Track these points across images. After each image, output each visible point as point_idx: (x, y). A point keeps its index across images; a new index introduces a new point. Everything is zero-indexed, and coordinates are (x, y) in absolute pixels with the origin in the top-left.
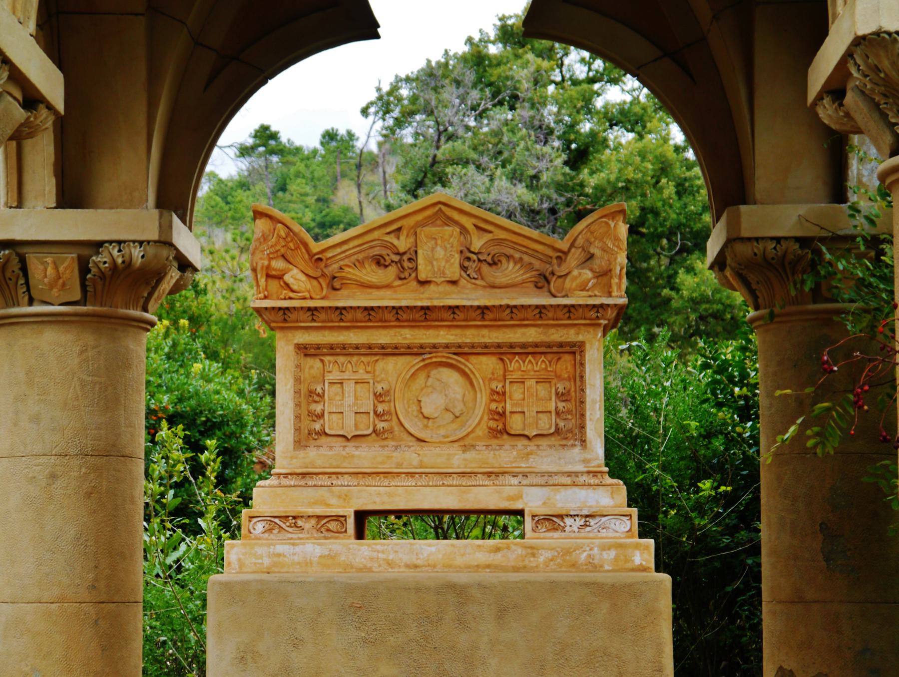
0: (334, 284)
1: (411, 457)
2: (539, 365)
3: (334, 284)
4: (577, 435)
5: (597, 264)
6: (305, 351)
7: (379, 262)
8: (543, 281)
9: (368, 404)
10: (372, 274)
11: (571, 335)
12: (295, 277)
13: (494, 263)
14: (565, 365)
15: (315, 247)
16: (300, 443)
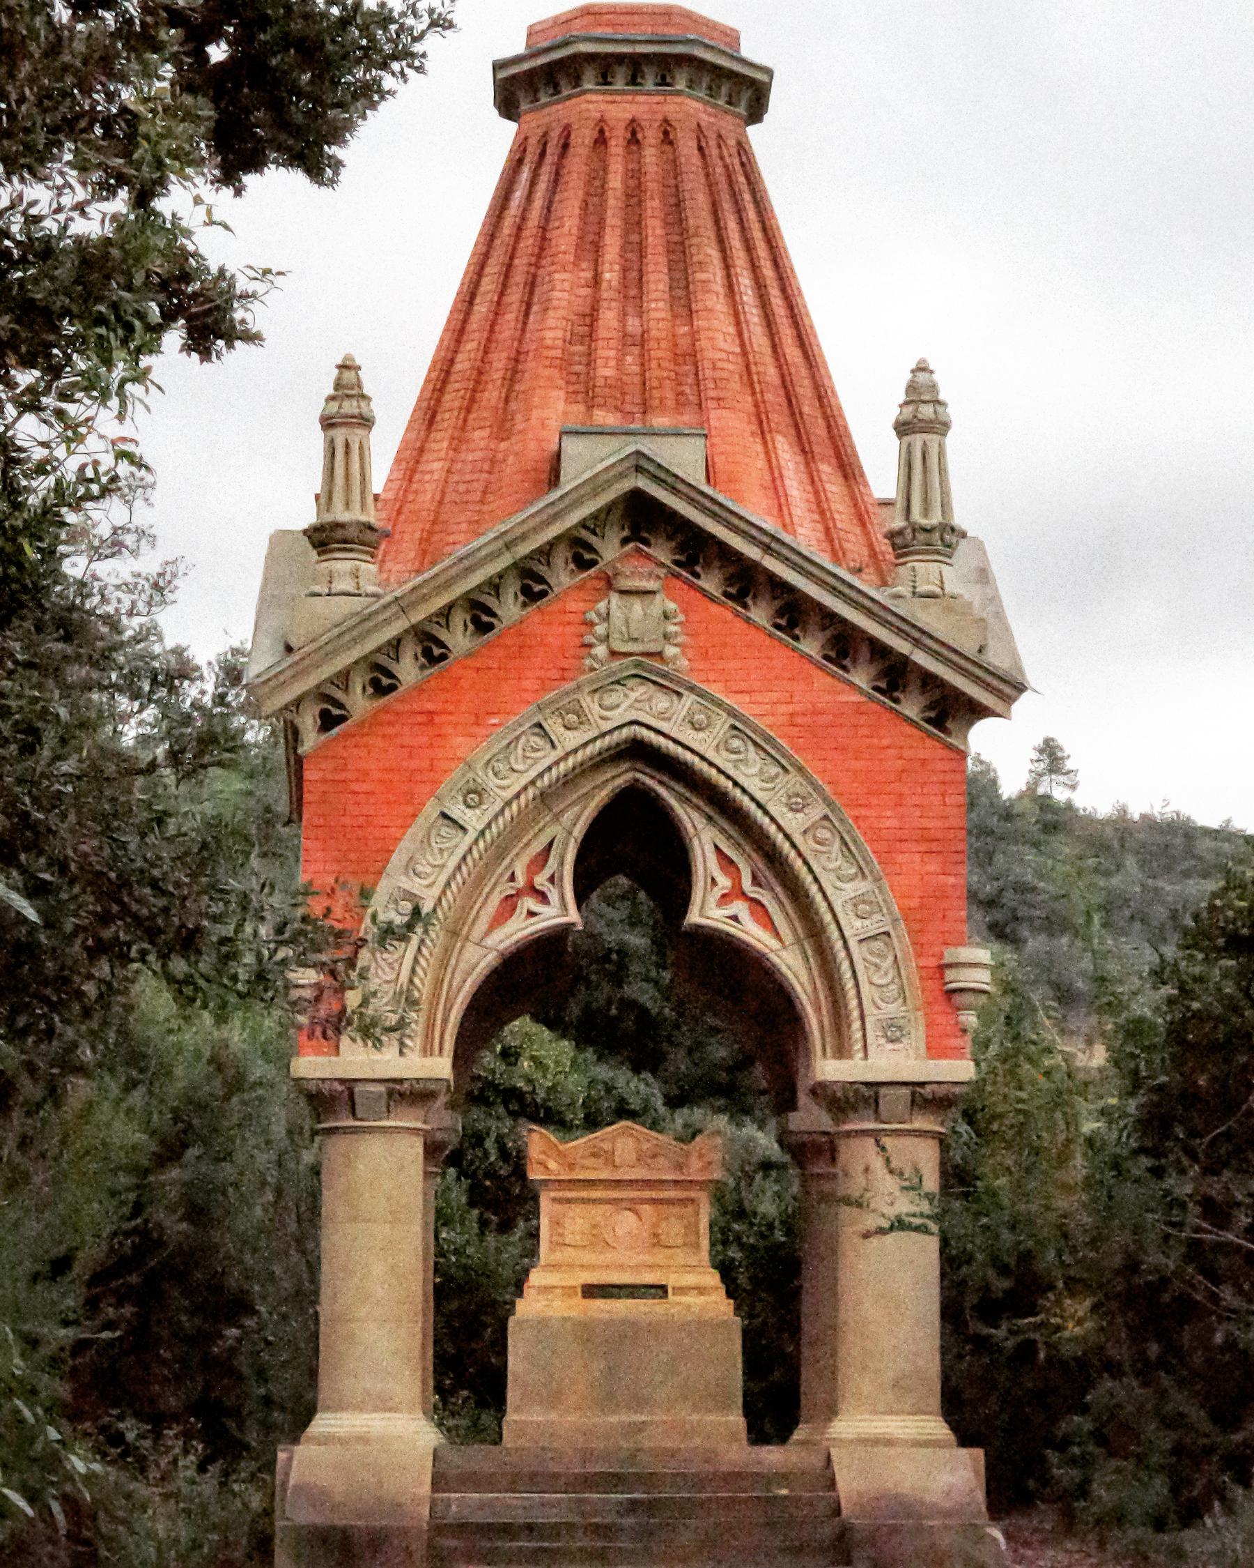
0: (571, 1166)
1: (609, 1256)
2: (675, 1210)
3: (571, 1166)
4: (697, 1246)
5: (707, 1159)
6: (554, 1200)
7: (594, 1155)
8: (679, 1167)
9: (587, 1228)
10: (590, 1162)
11: (693, 1194)
12: (552, 1165)
13: (654, 1156)
14: (690, 1209)
15: (561, 1147)
16: (552, 1250)
